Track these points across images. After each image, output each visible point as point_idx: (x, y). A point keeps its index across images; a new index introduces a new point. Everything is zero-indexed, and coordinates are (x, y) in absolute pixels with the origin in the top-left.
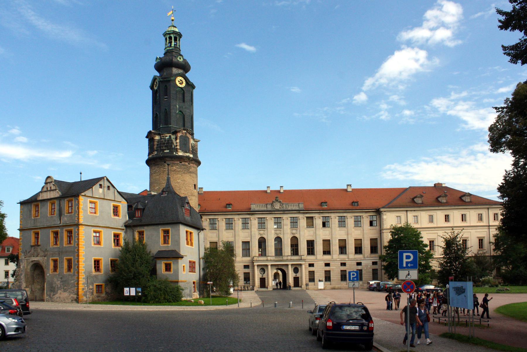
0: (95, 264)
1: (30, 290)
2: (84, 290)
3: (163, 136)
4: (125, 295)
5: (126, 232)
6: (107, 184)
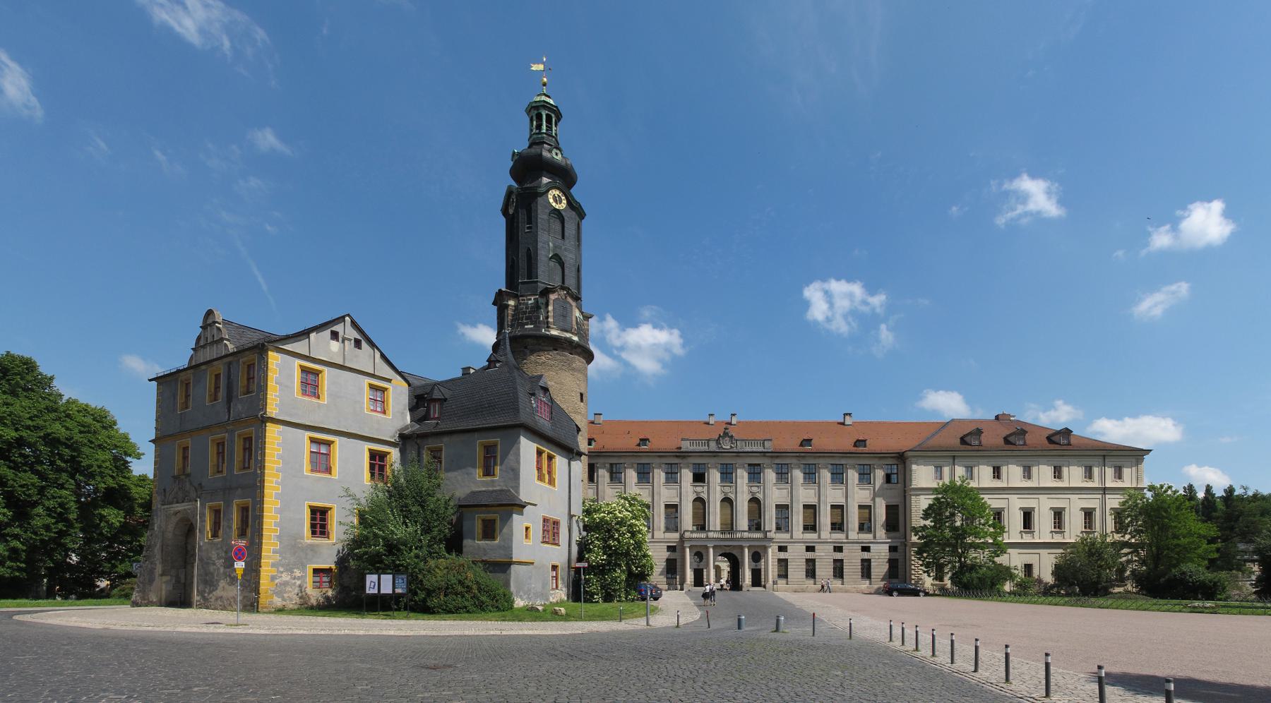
0: (313, 519)
1: (174, 581)
2: (277, 581)
3: (523, 300)
4: (368, 592)
5: (402, 452)
6: (353, 334)
